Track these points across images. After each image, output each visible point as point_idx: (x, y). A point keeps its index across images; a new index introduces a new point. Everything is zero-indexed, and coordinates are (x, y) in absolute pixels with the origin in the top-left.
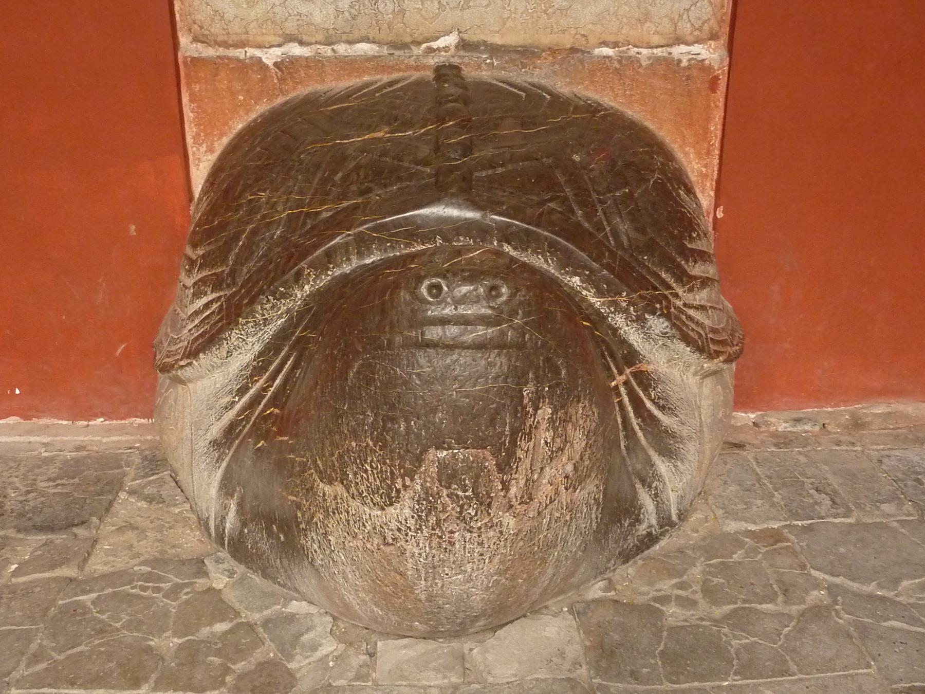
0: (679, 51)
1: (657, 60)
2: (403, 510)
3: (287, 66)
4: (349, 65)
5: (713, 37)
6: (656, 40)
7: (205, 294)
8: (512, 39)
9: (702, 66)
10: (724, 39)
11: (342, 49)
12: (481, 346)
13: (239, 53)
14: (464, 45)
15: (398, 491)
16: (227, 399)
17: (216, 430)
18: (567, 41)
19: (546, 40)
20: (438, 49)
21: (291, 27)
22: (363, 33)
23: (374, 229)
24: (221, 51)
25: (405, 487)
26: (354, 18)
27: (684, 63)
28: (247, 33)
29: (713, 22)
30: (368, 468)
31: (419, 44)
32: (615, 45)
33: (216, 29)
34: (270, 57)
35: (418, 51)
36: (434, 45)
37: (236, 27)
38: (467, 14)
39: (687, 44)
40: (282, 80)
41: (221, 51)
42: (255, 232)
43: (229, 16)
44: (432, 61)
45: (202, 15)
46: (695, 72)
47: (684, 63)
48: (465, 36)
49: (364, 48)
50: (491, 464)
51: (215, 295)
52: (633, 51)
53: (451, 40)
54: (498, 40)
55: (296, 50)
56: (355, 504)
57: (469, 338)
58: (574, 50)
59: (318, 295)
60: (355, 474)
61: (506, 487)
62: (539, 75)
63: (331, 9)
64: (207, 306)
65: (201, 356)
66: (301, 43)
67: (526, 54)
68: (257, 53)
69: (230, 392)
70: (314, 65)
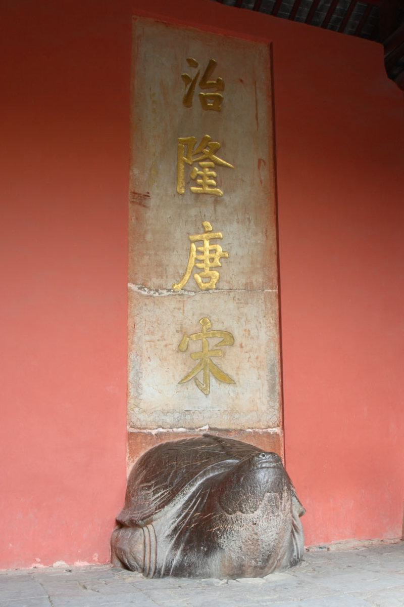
0: (269, 430)
1: (264, 433)
2: (258, 512)
3: (159, 435)
4: (177, 434)
5: (278, 426)
6: (263, 427)
7: (161, 491)
9: (276, 434)
10: (281, 426)
11: (175, 430)
12: (274, 467)
13: (145, 431)
14: (210, 429)
15: (258, 506)
16: (174, 520)
17: (168, 532)
18: (239, 428)
19: (233, 427)
20: (203, 430)
21: (160, 423)
22: (181, 425)
23: (216, 465)
24: (139, 430)
25: (260, 504)
26: (179, 421)
27: (272, 433)
28: (147, 425)
29: (278, 422)
30: (249, 501)
31: (197, 428)
32: (252, 428)
33: (138, 424)
34: (154, 432)
35: (197, 430)
36: (202, 429)
37: (144, 423)
38: (211, 419)
39: (271, 428)
40: (157, 439)
41: (139, 430)
42: (176, 472)
43: (142, 420)
44: (202, 433)
45: (134, 420)
46: (275, 436)
47: (272, 433)
48: (210, 426)
50: (278, 497)
51: (164, 491)
52: (257, 430)
53: (207, 427)
54: (220, 427)
55: (161, 430)
56: (243, 515)
57: (272, 466)
58: (241, 430)
59: (202, 484)
60: (245, 505)
61: (281, 505)
62: (232, 437)
63: (172, 418)
64: (163, 494)
65: (166, 507)
66: (163, 428)
67: (227, 431)
68: (150, 431)
69: (174, 518)
70: (167, 434)
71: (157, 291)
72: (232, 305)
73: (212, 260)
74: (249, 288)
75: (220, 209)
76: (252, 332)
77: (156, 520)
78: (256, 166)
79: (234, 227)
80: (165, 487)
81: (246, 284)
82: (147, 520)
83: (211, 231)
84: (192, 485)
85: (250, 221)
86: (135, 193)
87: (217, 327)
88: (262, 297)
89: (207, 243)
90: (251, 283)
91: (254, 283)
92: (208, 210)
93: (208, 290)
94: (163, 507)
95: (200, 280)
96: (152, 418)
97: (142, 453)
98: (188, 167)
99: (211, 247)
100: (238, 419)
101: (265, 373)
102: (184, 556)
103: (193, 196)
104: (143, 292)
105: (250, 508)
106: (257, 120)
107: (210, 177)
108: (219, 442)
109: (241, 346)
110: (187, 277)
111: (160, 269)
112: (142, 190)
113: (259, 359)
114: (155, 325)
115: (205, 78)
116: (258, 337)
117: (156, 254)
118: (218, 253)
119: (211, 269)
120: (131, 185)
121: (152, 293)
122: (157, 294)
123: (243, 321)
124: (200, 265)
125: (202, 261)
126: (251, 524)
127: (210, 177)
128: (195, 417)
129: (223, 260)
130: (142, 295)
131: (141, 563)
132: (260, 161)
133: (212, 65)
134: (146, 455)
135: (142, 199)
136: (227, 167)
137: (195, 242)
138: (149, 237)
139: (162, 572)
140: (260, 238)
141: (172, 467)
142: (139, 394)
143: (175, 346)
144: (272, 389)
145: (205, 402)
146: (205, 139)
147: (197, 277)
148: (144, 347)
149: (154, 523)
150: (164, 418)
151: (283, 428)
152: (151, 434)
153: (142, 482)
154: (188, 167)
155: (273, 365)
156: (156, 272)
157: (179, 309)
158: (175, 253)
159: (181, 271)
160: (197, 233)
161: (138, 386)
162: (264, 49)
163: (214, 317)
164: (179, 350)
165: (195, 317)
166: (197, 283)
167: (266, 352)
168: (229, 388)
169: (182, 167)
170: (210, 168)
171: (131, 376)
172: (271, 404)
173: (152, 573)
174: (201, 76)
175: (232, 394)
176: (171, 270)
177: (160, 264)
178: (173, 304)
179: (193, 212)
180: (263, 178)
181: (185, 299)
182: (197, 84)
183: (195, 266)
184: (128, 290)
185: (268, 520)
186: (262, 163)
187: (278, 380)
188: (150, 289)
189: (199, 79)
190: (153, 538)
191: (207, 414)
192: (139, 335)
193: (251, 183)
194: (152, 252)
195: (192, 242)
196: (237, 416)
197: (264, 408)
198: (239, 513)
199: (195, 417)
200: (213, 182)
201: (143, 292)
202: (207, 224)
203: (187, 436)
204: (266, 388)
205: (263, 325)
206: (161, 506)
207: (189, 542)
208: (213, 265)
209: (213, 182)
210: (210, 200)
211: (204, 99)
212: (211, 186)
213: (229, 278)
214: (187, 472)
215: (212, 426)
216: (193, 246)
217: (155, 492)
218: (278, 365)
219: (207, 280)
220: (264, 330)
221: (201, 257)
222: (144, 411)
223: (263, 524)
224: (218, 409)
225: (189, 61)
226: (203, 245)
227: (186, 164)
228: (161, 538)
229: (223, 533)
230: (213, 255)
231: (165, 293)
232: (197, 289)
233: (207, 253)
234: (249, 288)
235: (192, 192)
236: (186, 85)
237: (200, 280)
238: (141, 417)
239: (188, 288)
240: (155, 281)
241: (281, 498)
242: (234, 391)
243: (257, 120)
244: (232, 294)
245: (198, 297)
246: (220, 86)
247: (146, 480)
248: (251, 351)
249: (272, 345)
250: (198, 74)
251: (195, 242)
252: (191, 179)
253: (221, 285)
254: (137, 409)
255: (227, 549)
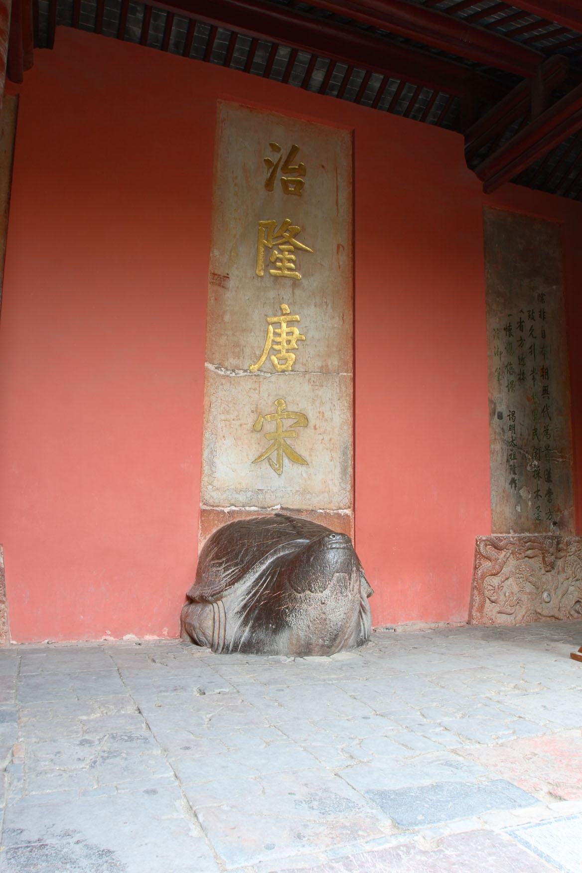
0: (340, 511)
2: (327, 592)
4: (249, 513)
8: (295, 507)
9: (347, 515)
11: (247, 508)
12: (344, 548)
14: (282, 508)
19: (305, 507)
21: (233, 501)
33: (211, 501)
34: (226, 510)
37: (217, 501)
42: (247, 549)
44: (274, 513)
45: (207, 497)
49: (253, 508)
53: (279, 507)
54: (291, 507)
55: (233, 508)
56: (312, 594)
59: (272, 562)
62: (303, 517)
70: (240, 512)
71: (234, 371)
72: (307, 387)
73: (289, 342)
74: (325, 371)
75: (298, 292)
76: (325, 415)
77: (226, 596)
78: (335, 251)
79: (311, 311)
80: (236, 565)
81: (322, 367)
82: (217, 596)
83: (288, 314)
84: (262, 564)
85: (327, 305)
86: (214, 274)
87: (292, 408)
88: (337, 380)
89: (284, 325)
90: (327, 366)
91: (330, 366)
92: (286, 293)
93: (283, 371)
94: (233, 584)
95: (276, 361)
96: (224, 496)
97: (214, 531)
98: (268, 250)
99: (288, 330)
100: (309, 500)
101: (338, 455)
102: (253, 633)
103: (272, 279)
104: (219, 372)
105: (319, 587)
106: (337, 204)
107: (290, 260)
108: (290, 521)
109: (315, 428)
110: (264, 358)
111: (238, 349)
112: (221, 272)
113: (333, 441)
114: (231, 405)
115: (287, 162)
116: (332, 419)
117: (233, 335)
118: (295, 336)
119: (288, 351)
120: (211, 267)
121: (229, 372)
122: (234, 374)
123: (317, 403)
124: (276, 347)
125: (279, 343)
126: (319, 603)
127: (290, 260)
128: (267, 496)
129: (299, 342)
130: (218, 375)
131: (210, 639)
132: (338, 246)
133: (294, 150)
134: (218, 532)
135: (221, 280)
136: (306, 251)
137: (272, 324)
138: (227, 318)
139: (230, 649)
140: (337, 322)
141: (243, 544)
142: (213, 472)
143: (249, 426)
144: (344, 471)
145: (277, 482)
146: (285, 223)
147: (274, 358)
148: (219, 426)
149: (223, 600)
150: (237, 496)
151: (354, 510)
152: (223, 512)
153: (213, 559)
154: (268, 250)
155: (346, 448)
156: (233, 352)
157: (255, 389)
158: (252, 334)
159: (257, 353)
160: (275, 316)
161: (212, 464)
162: (346, 136)
163: (289, 399)
164: (254, 430)
165: (271, 398)
166: (273, 365)
167: (339, 435)
168: (302, 469)
169: (262, 249)
170: (290, 252)
171: (206, 453)
172: (343, 485)
173: (220, 649)
174: (283, 160)
175: (304, 475)
176: (248, 351)
177: (237, 345)
178: (249, 384)
179: (272, 294)
180: (341, 263)
181: (261, 379)
182: (279, 169)
183: (272, 348)
184: (204, 370)
185: (337, 600)
186: (341, 249)
187: (350, 462)
188: (227, 370)
189: (282, 164)
190: (222, 615)
191: (279, 494)
192: (215, 413)
193: (330, 269)
194: (230, 333)
195: (269, 324)
196: (308, 496)
197: (335, 489)
198: (308, 592)
199: (267, 496)
200: (292, 265)
201: (219, 372)
202: (285, 306)
203: (259, 514)
204: (338, 470)
205: (338, 408)
206: (232, 583)
207: (257, 619)
208: (289, 347)
209: (292, 265)
210: (289, 283)
211: (285, 184)
212: (290, 269)
213: (305, 361)
214: (257, 550)
215: (284, 506)
216: (271, 328)
217: (226, 569)
218: (351, 448)
219: (283, 362)
220: (338, 413)
221: (278, 339)
222: (218, 489)
223: (331, 603)
224: (289, 489)
225: (271, 145)
226: (281, 327)
227: (266, 247)
228: (231, 615)
229: (291, 612)
230: (289, 338)
231: (241, 373)
232: (273, 370)
233: (284, 335)
234: (325, 371)
235: (271, 275)
236: (268, 169)
237: (276, 361)
238: (214, 494)
239: (264, 369)
240: (232, 361)
241: (350, 579)
242: (306, 472)
243: (337, 204)
244: (307, 377)
245: (273, 379)
246: (302, 171)
247: (217, 557)
248: (324, 433)
249: (345, 427)
250: (281, 158)
251: (272, 324)
252: (271, 262)
253: (297, 367)
254: (210, 487)
255: (295, 627)
